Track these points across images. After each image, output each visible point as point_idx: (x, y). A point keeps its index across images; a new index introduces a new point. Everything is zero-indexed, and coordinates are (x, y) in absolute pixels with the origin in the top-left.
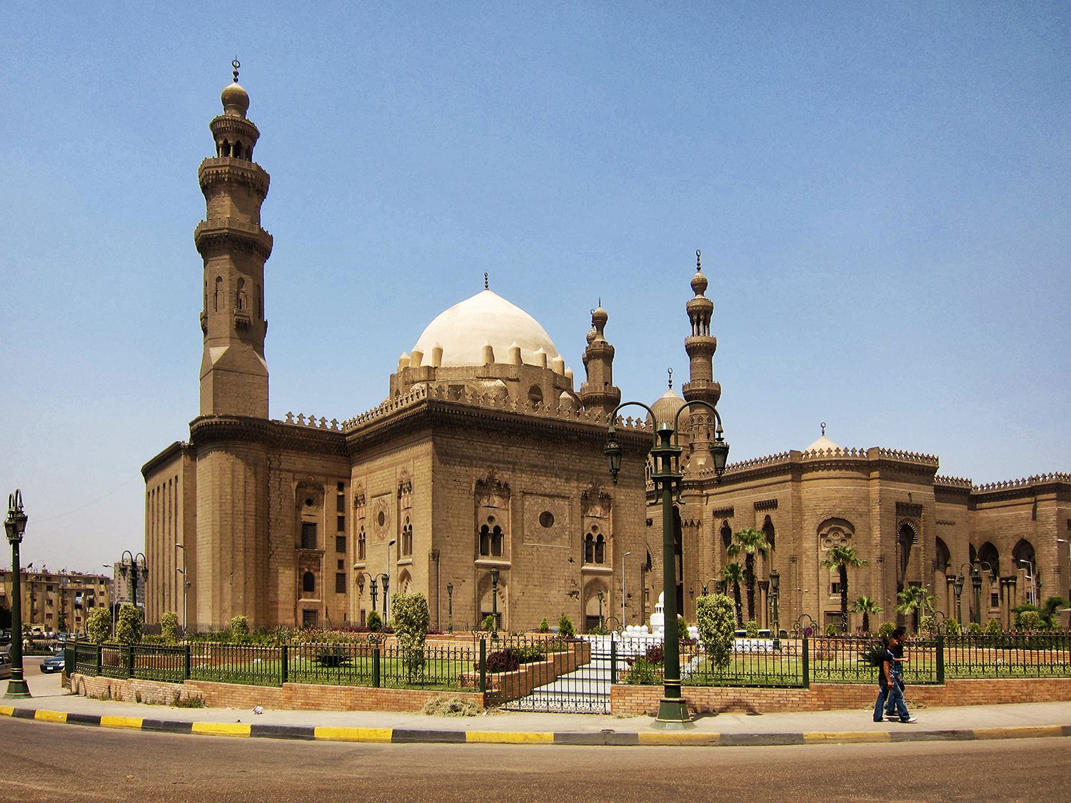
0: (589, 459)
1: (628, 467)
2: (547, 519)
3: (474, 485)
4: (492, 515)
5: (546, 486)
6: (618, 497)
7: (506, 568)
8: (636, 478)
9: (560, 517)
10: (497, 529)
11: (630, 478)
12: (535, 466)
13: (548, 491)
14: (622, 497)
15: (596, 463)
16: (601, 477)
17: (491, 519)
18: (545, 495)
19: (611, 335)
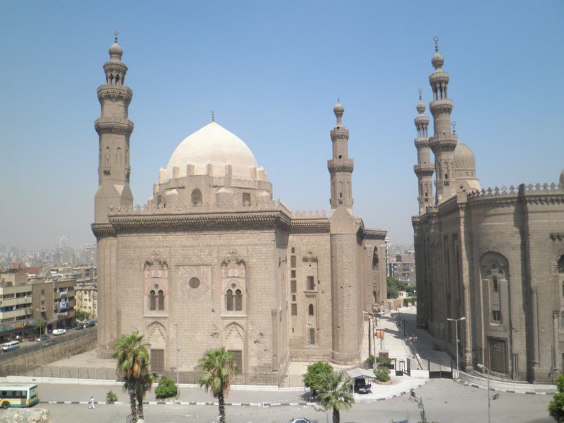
0: (227, 235)
1: (259, 237)
2: (195, 283)
3: (143, 266)
4: (157, 283)
5: (193, 259)
6: (250, 260)
7: (165, 318)
8: (266, 245)
9: (205, 280)
10: (161, 292)
11: (262, 245)
12: (185, 246)
13: (195, 263)
14: (255, 260)
15: (233, 238)
16: (236, 248)
17: (157, 286)
18: (193, 265)
19: (345, 123)
